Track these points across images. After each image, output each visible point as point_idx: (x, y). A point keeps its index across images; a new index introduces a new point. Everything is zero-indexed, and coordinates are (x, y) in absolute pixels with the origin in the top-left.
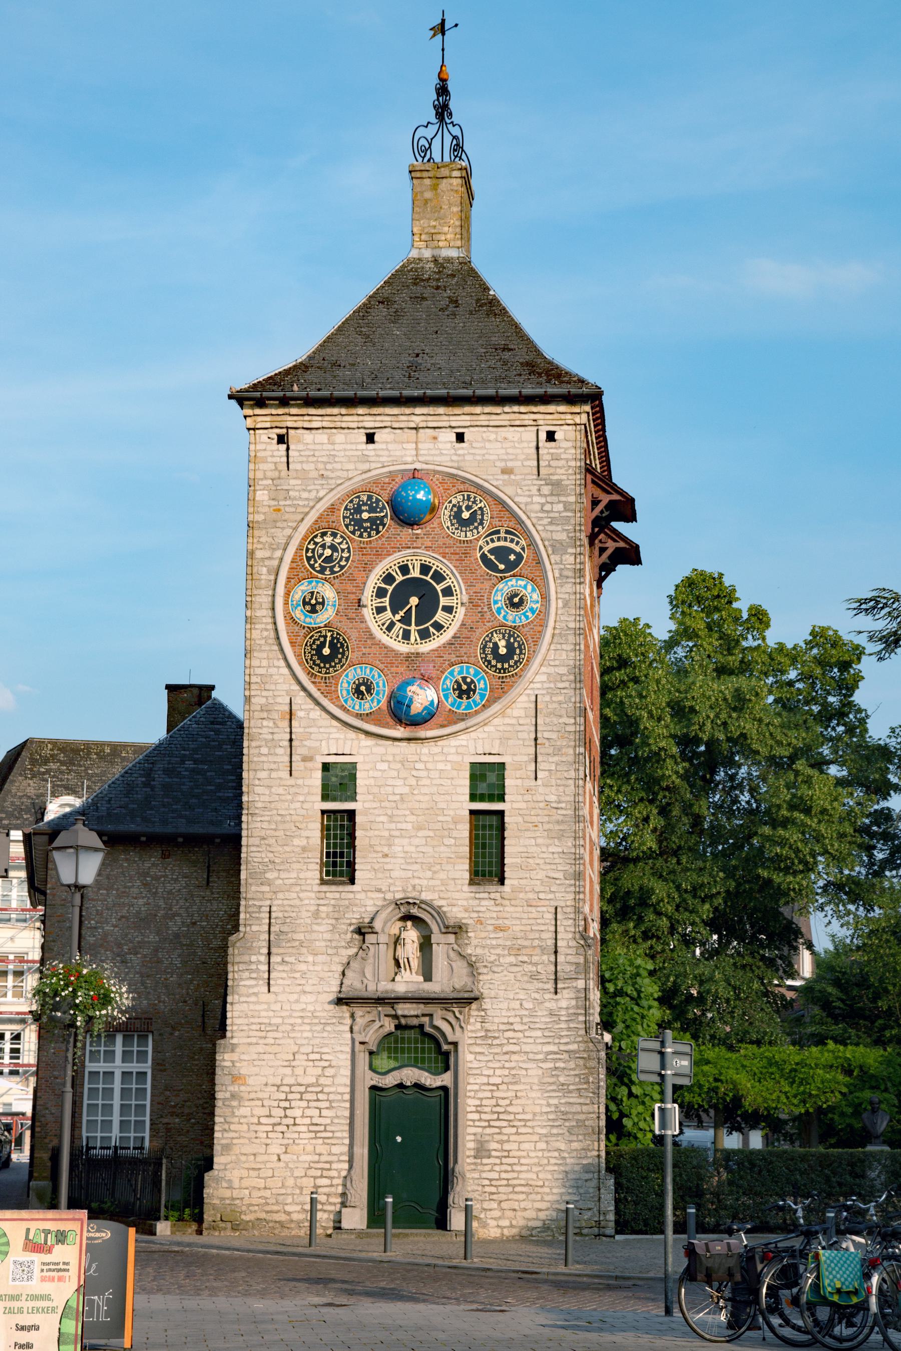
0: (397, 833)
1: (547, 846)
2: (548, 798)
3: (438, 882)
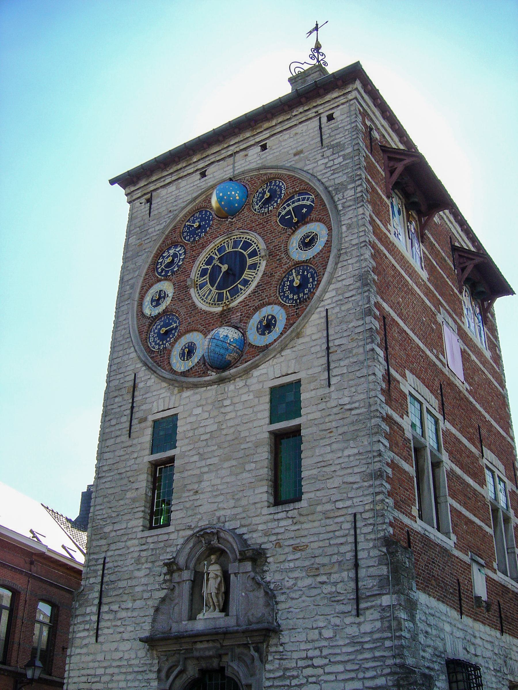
0: (206, 469)
1: (343, 451)
2: (341, 402)
3: (240, 510)
